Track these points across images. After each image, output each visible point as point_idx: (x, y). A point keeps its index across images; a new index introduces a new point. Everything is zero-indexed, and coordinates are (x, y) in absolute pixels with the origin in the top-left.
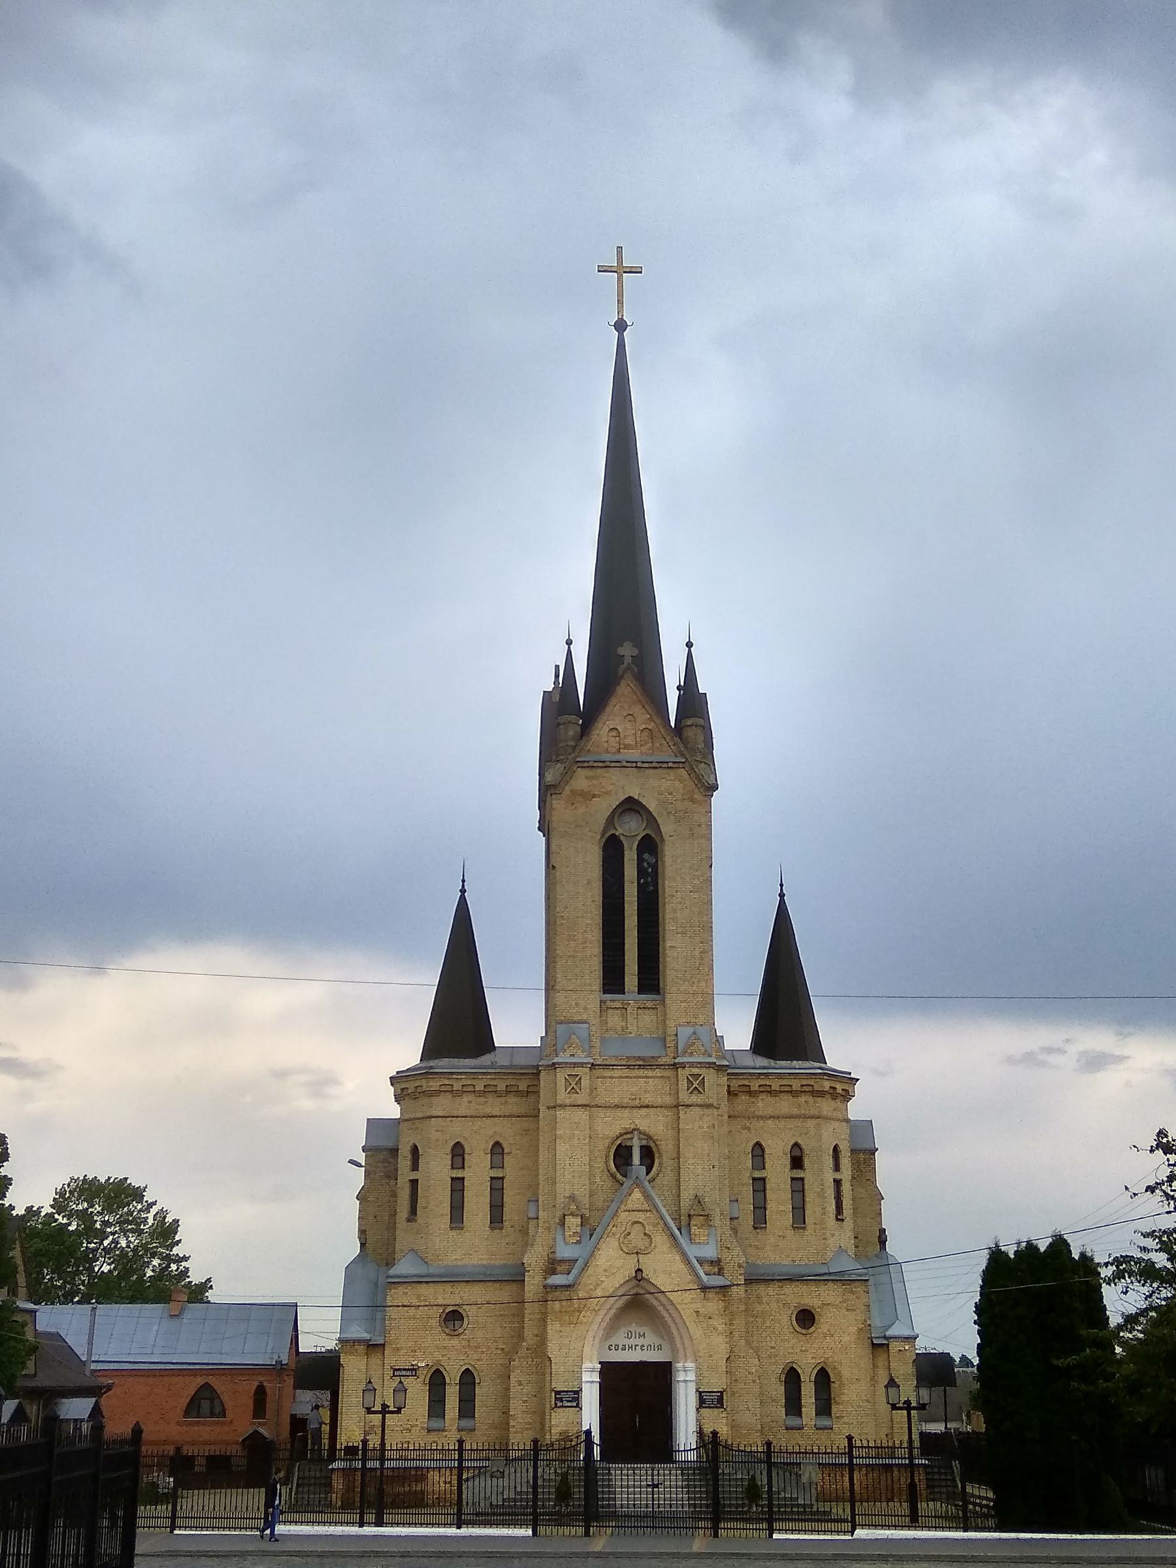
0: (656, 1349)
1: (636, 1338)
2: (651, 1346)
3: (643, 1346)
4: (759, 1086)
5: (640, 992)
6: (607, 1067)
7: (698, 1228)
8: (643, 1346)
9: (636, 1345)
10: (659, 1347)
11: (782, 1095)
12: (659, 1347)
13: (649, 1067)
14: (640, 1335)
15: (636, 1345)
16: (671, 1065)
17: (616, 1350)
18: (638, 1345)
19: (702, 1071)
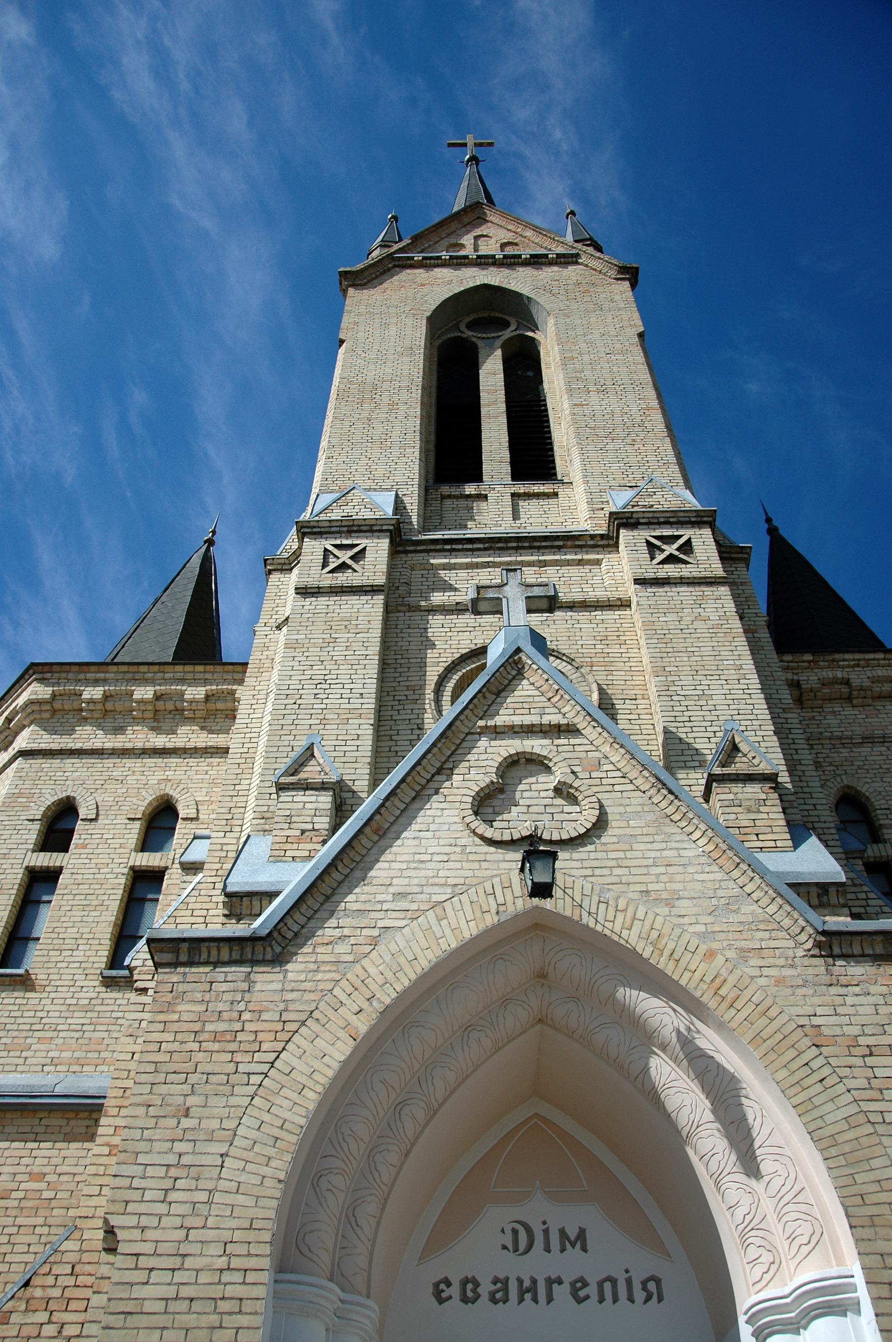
0: (639, 1295)
1: (548, 1249)
2: (613, 1281)
3: (585, 1284)
4: (824, 683)
5: (514, 478)
6: (438, 547)
7: (749, 811)
8: (578, 1287)
9: (550, 1282)
10: (652, 1286)
11: (879, 704)
12: (652, 1286)
13: (544, 544)
14: (563, 1233)
15: (550, 1282)
16: (602, 536)
17: (465, 1300)
18: (560, 1282)
19: (686, 533)
